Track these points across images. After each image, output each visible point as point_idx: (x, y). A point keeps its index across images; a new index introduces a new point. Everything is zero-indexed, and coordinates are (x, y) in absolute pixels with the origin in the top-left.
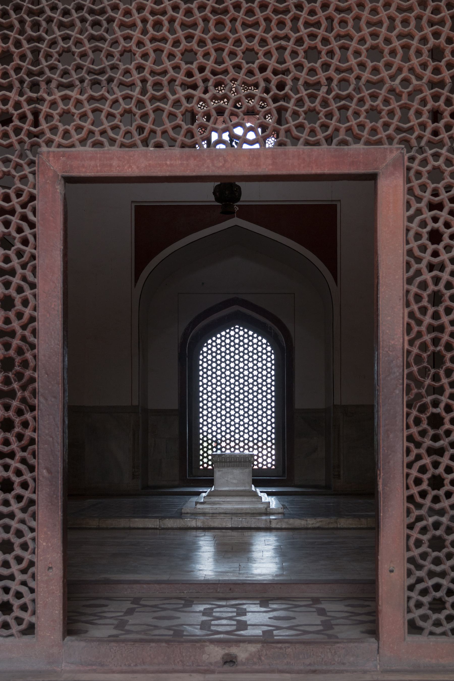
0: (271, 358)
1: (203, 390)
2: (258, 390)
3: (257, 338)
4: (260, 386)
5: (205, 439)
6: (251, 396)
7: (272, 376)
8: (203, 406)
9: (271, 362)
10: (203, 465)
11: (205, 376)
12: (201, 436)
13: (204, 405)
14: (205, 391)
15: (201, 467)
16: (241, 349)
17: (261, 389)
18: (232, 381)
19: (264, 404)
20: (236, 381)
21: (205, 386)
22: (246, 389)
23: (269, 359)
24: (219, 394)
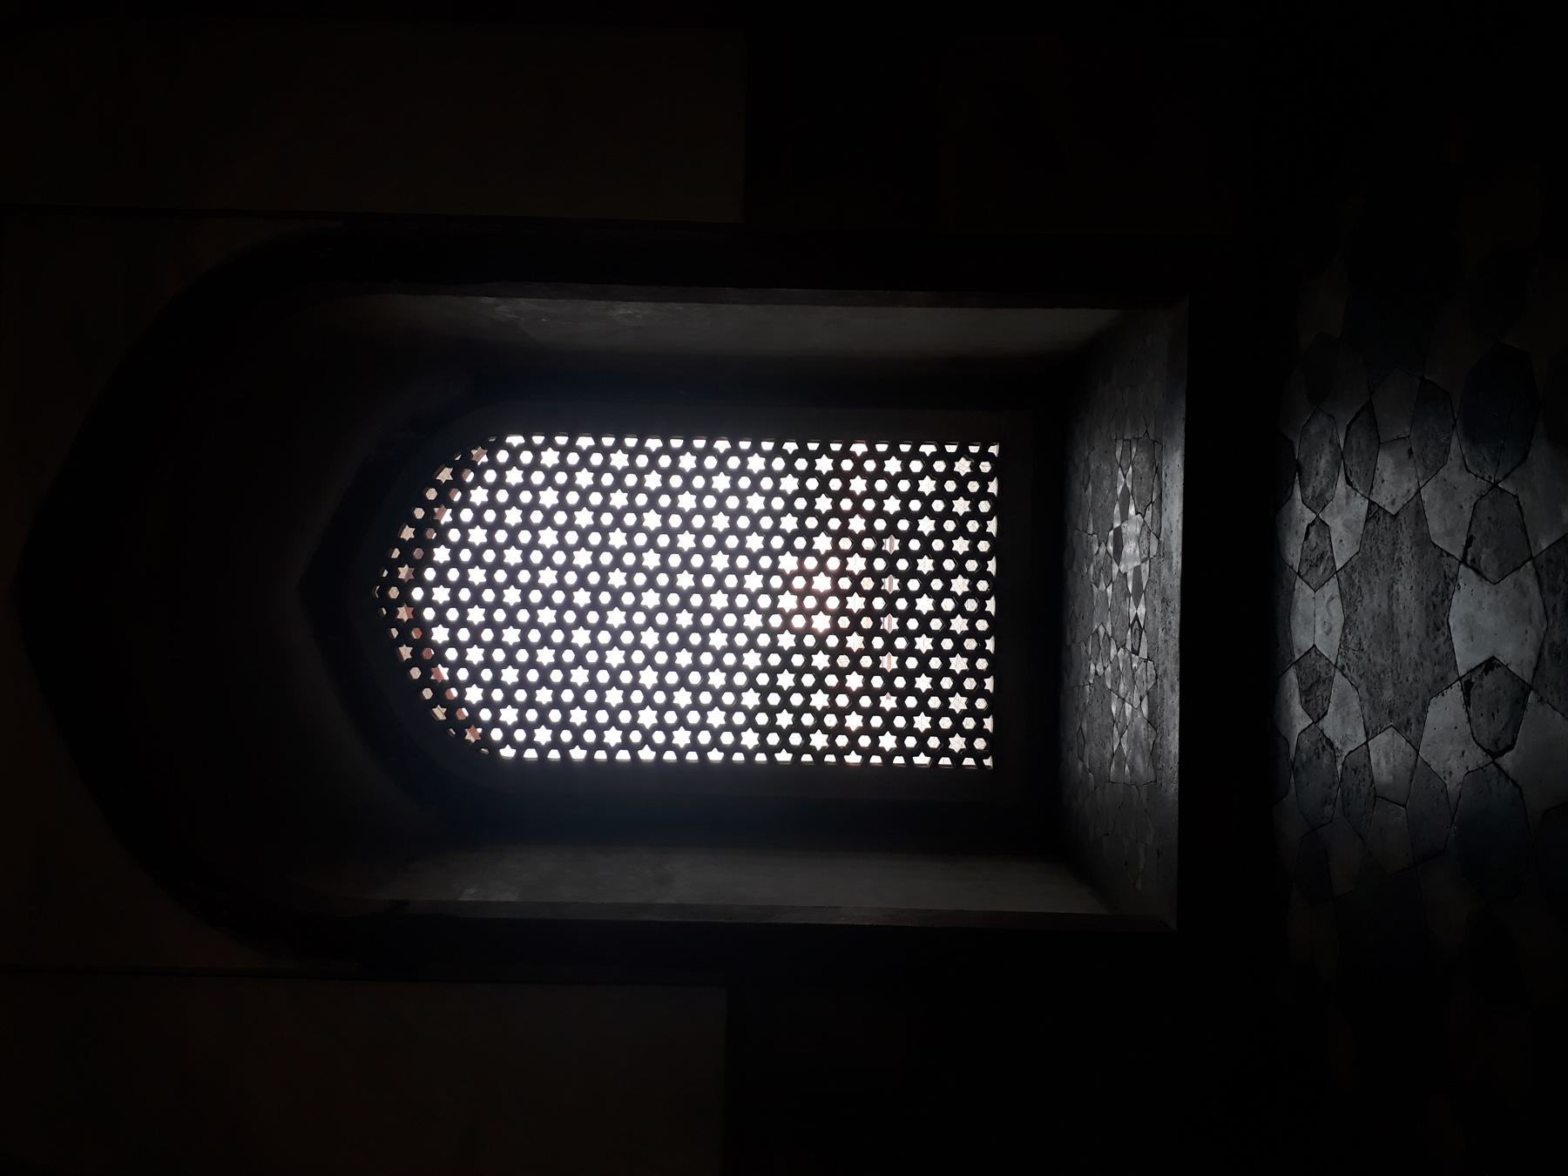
0: (521, 448)
1: (653, 747)
2: (659, 510)
3: (428, 506)
4: (641, 500)
5: (865, 741)
6: (686, 541)
7: (598, 448)
8: (721, 748)
9: (537, 451)
10: (979, 756)
11: (590, 736)
12: (853, 758)
13: (716, 743)
14: (659, 737)
15: (988, 762)
16: (477, 576)
17: (653, 497)
18: (616, 618)
19: (721, 482)
20: (616, 602)
21: (636, 737)
22: (651, 560)
23: (526, 457)
24: (672, 678)
